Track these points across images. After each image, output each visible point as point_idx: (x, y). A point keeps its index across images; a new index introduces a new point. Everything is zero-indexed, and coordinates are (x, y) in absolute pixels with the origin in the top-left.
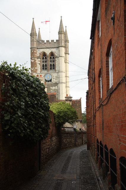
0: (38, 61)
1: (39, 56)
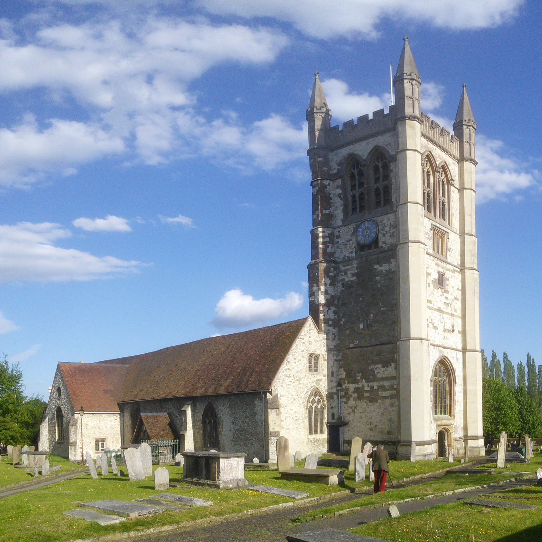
0: (334, 190)
1: (338, 170)
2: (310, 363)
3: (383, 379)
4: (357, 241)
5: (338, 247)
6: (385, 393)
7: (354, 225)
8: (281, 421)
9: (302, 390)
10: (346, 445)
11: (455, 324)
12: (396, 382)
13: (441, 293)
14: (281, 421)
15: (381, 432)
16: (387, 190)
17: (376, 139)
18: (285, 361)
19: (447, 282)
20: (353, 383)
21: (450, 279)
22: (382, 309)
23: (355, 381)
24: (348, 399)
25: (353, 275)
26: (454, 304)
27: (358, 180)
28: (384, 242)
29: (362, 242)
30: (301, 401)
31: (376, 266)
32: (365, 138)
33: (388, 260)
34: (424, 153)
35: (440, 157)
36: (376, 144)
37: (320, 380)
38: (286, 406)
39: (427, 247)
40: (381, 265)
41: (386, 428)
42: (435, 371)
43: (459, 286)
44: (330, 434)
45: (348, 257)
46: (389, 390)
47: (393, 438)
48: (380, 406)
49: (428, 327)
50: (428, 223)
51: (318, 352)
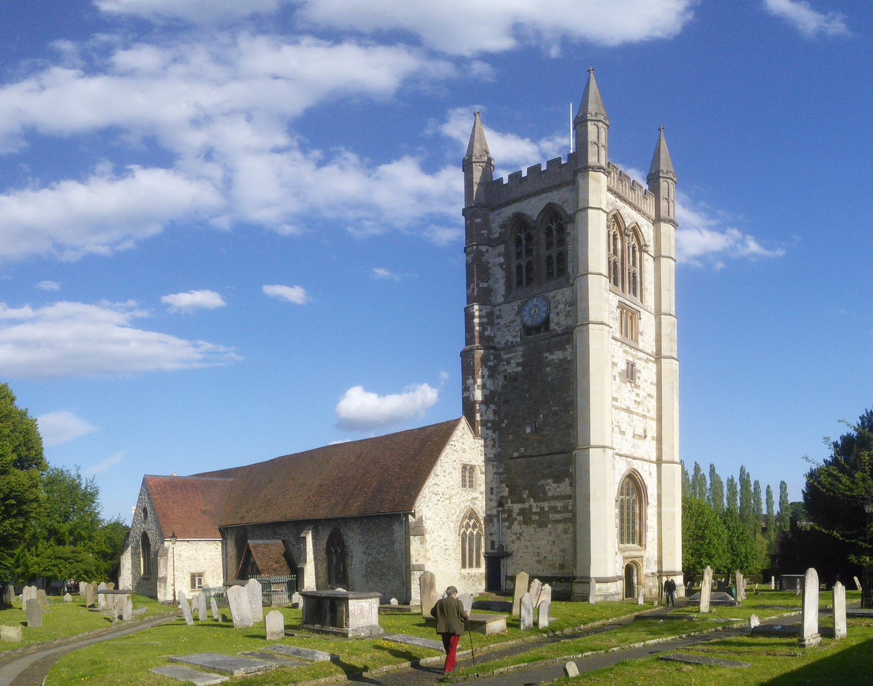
0: (495, 257)
2: (464, 476)
3: (555, 498)
4: (522, 322)
5: (499, 329)
6: (557, 517)
7: (519, 302)
8: (427, 551)
9: (453, 511)
10: (509, 582)
11: (648, 429)
12: (571, 502)
13: (630, 389)
14: (427, 551)
15: (552, 565)
16: (562, 258)
17: (550, 194)
18: (432, 475)
19: (638, 374)
20: (518, 502)
21: (642, 371)
22: (553, 409)
23: (521, 501)
24: (511, 523)
25: (518, 365)
26: (646, 402)
27: (526, 246)
28: (558, 324)
29: (529, 323)
30: (452, 525)
31: (546, 355)
32: (537, 193)
33: (562, 347)
34: (611, 211)
35: (630, 216)
36: (549, 201)
37: (476, 499)
38: (433, 532)
39: (613, 329)
40: (552, 353)
41: (558, 560)
42: (622, 488)
43: (654, 379)
44: (488, 568)
45: (512, 342)
46: (562, 512)
47: (566, 573)
48: (550, 533)
49: (613, 431)
50: (614, 300)
51: (473, 463)
